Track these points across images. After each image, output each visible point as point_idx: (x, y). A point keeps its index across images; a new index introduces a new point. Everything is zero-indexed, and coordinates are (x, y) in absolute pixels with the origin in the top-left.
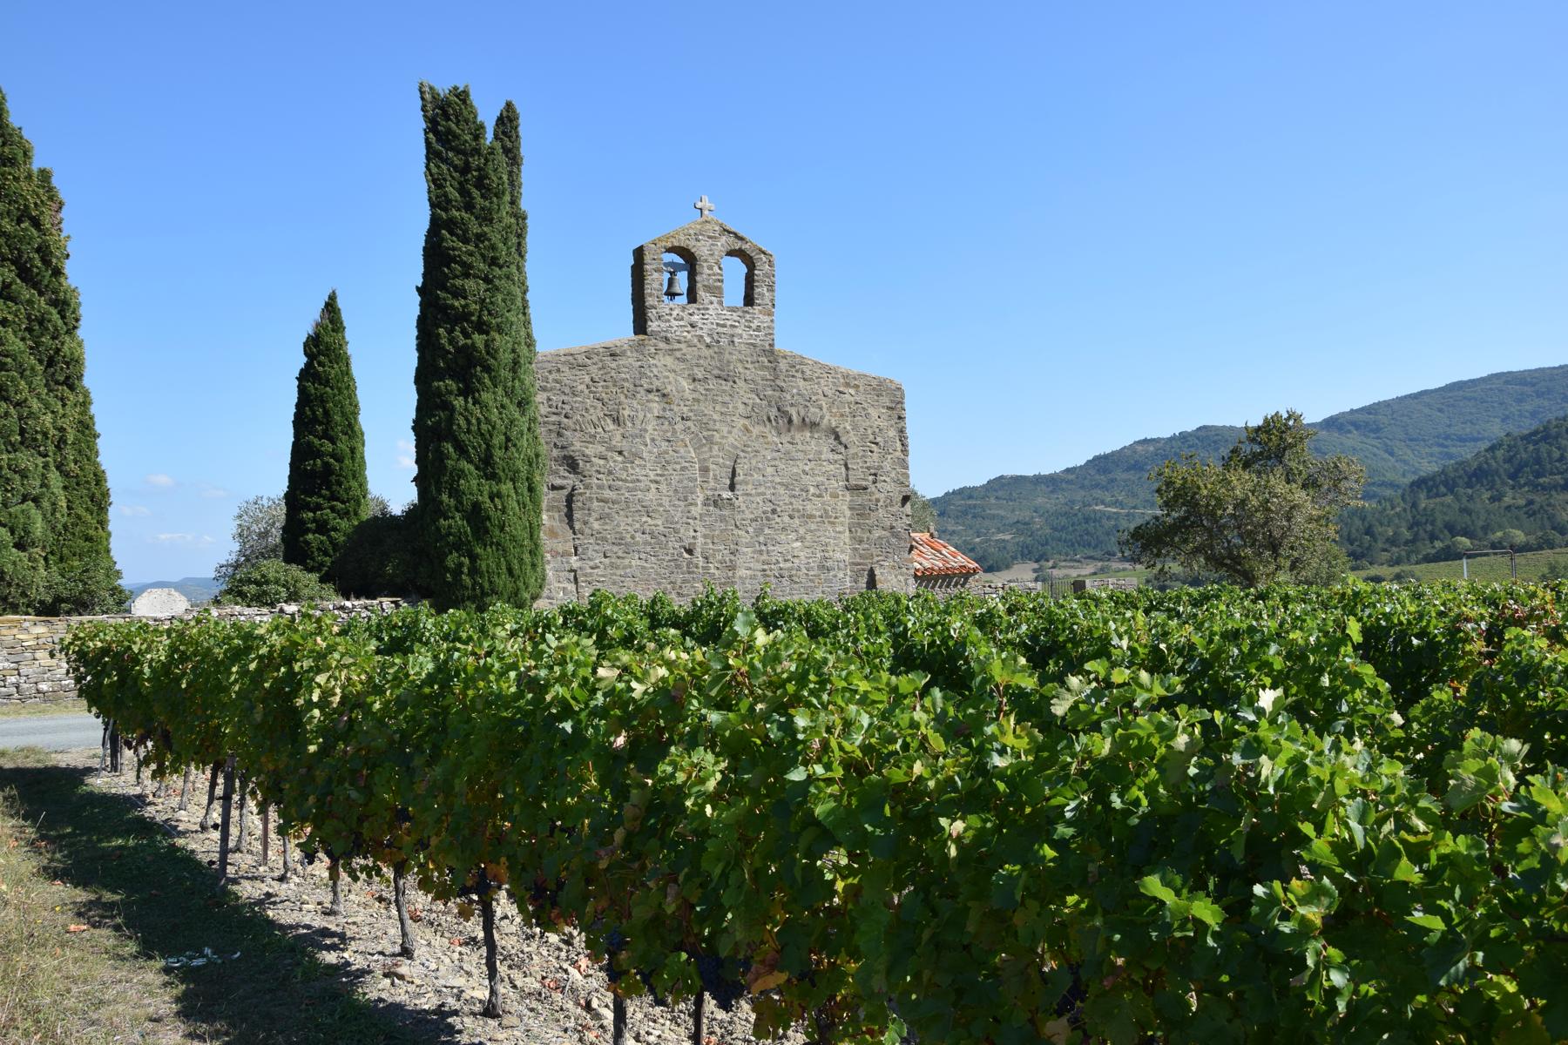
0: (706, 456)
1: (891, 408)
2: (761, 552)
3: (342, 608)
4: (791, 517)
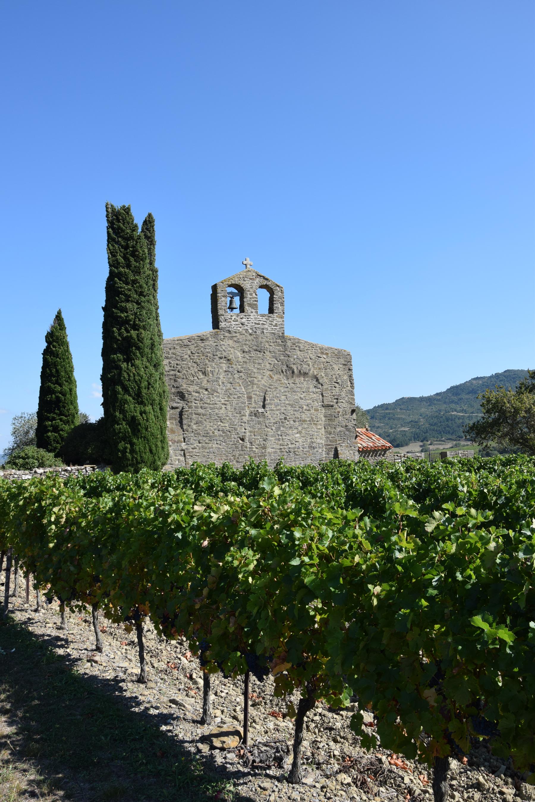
0: (250, 391)
1: (344, 365)
3: (66, 471)
4: (294, 421)
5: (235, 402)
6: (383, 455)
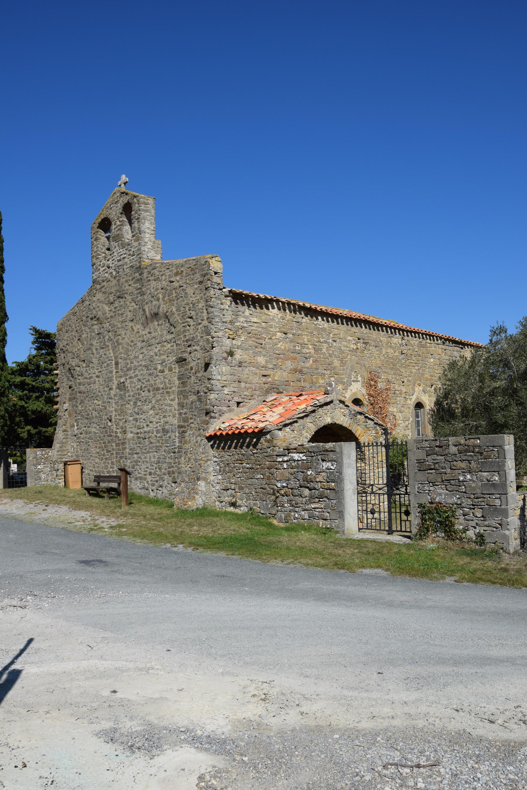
1: (201, 282)
2: (136, 420)
4: (149, 391)
6: (255, 446)
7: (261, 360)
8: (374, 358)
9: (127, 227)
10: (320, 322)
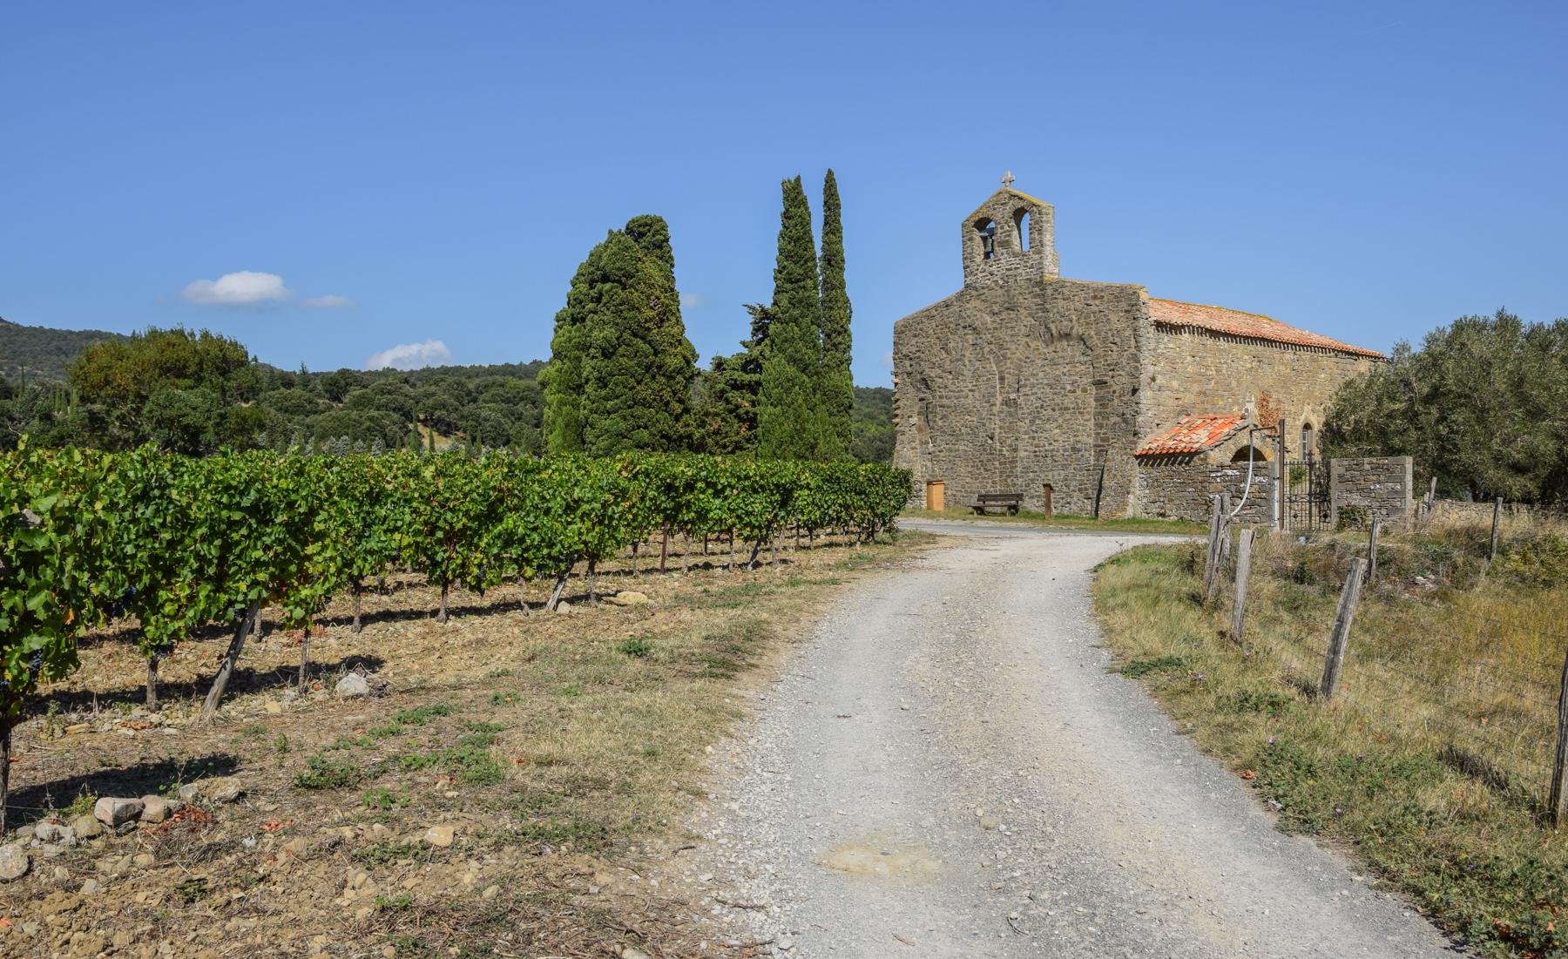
5: (983, 387)
7: (1175, 384)
8: (1267, 377)
9: (1015, 233)
10: (1223, 343)
